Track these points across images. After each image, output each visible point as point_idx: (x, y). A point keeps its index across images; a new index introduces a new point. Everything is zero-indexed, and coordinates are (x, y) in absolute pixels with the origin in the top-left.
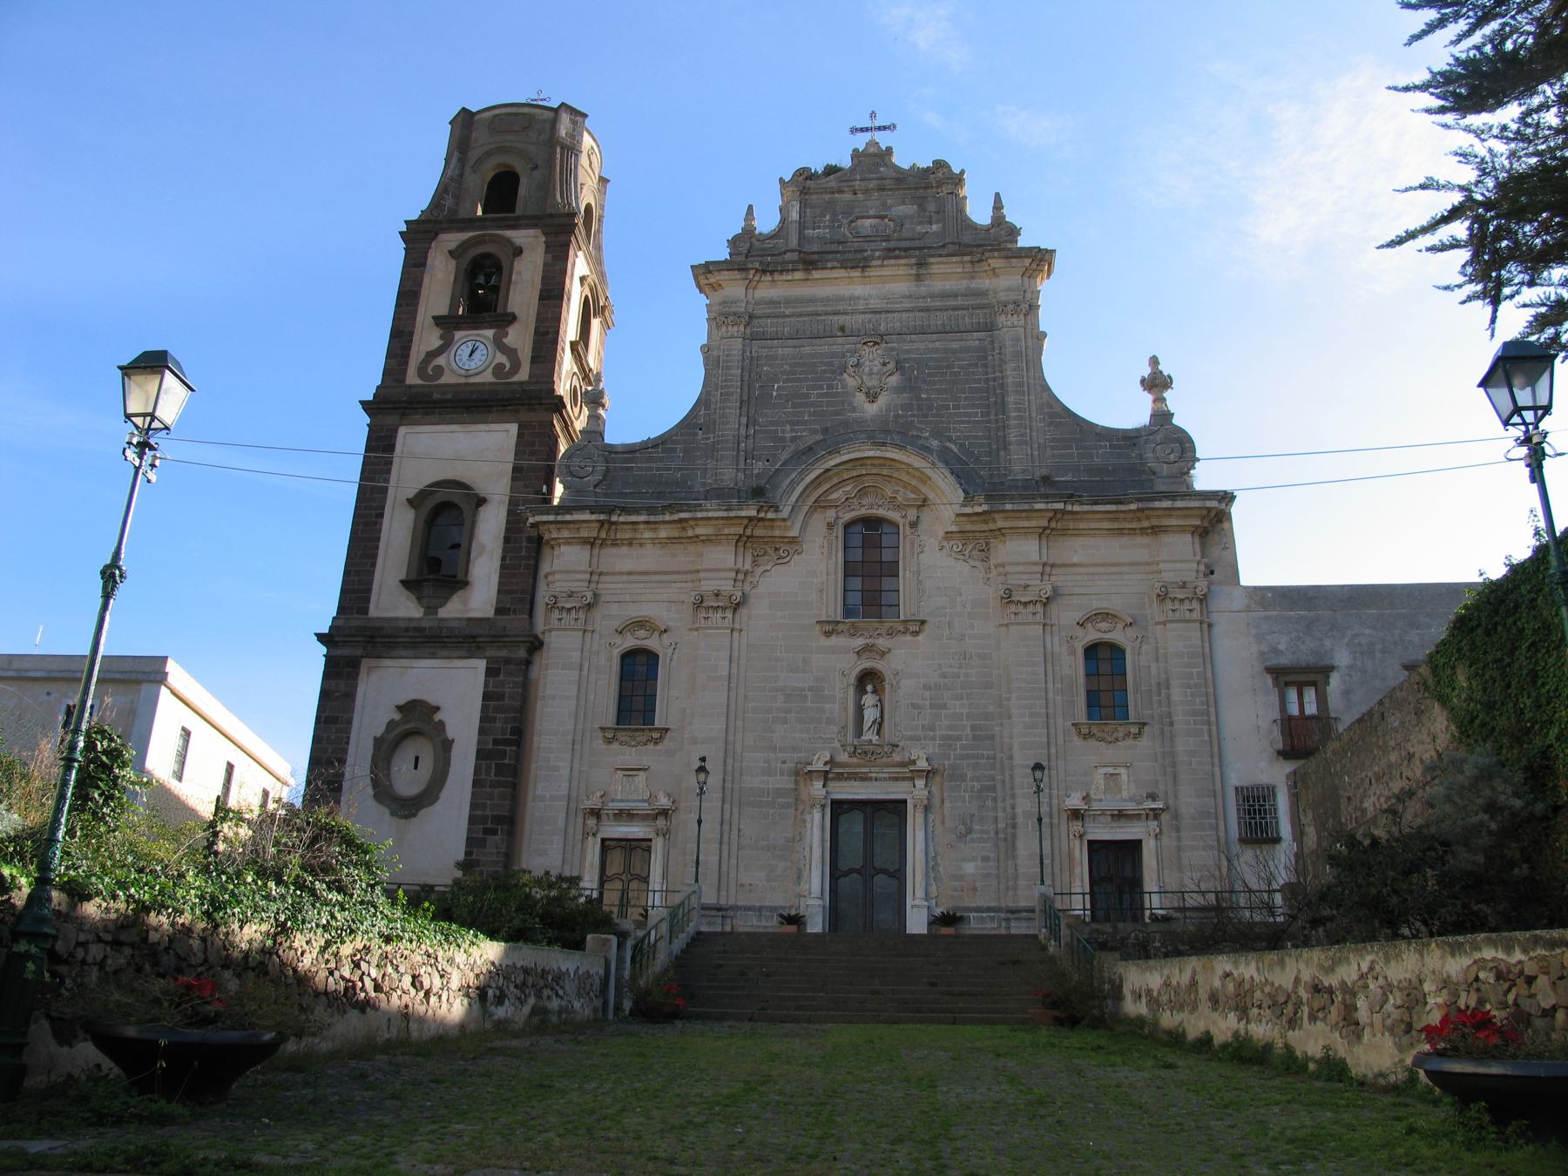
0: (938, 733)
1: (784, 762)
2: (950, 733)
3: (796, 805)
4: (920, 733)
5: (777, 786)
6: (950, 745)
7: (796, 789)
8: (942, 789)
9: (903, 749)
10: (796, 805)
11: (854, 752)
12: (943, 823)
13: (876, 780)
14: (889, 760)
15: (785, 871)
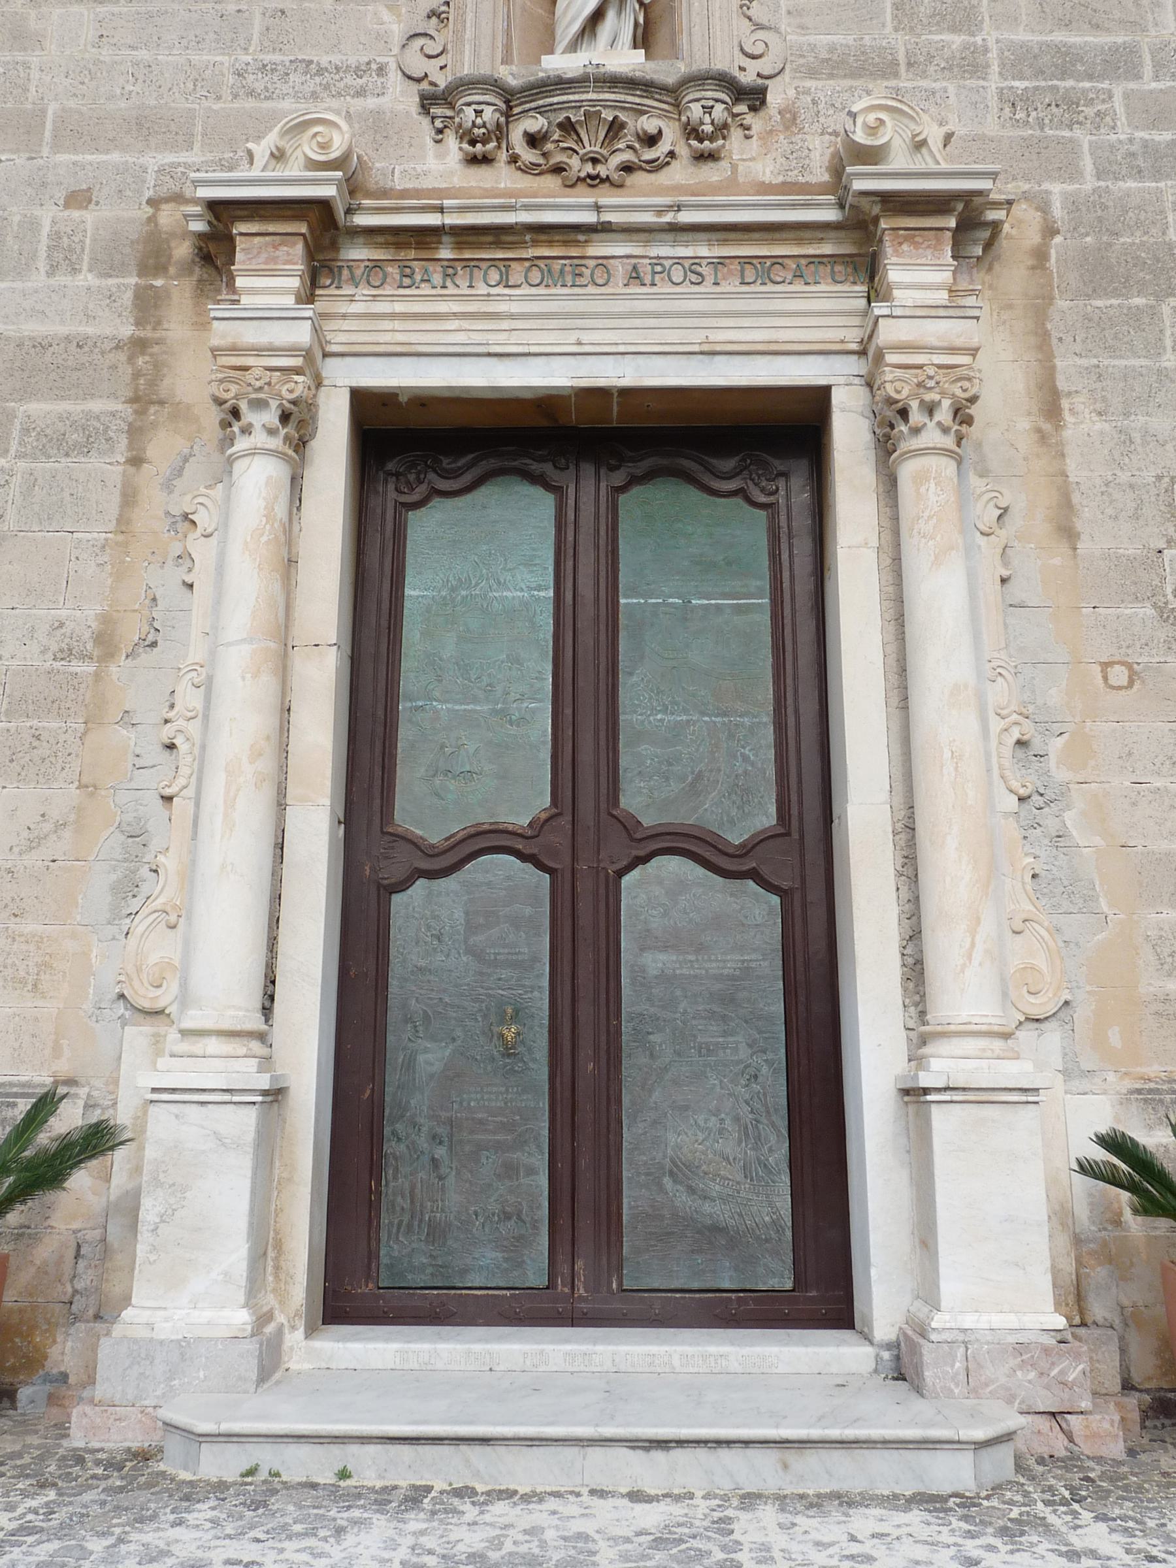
0: (989, 36)
1: (78, 199)
2: (1059, 37)
3: (136, 433)
4: (900, 43)
5: (33, 328)
6: (1071, 102)
7: (139, 345)
8: (1043, 344)
9: (790, 118)
10: (136, 433)
11: (500, 133)
12: (1068, 533)
13: (635, 276)
14: (711, 173)
15: (34, 844)
